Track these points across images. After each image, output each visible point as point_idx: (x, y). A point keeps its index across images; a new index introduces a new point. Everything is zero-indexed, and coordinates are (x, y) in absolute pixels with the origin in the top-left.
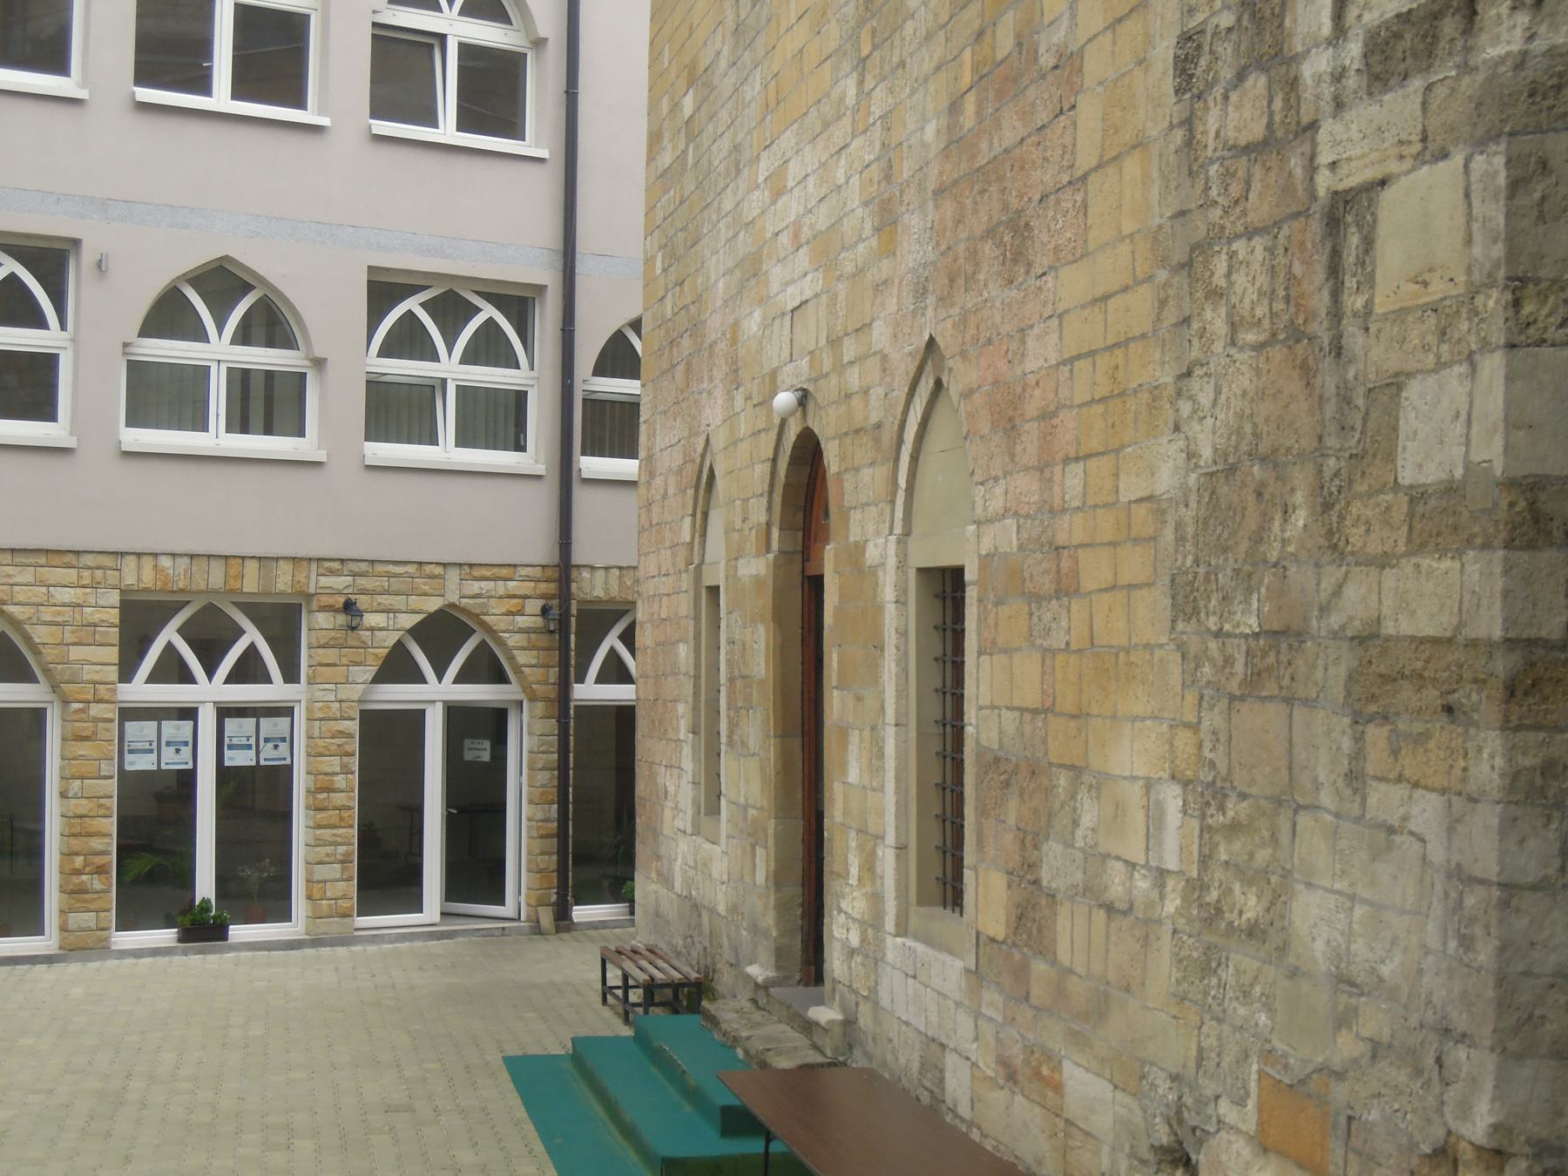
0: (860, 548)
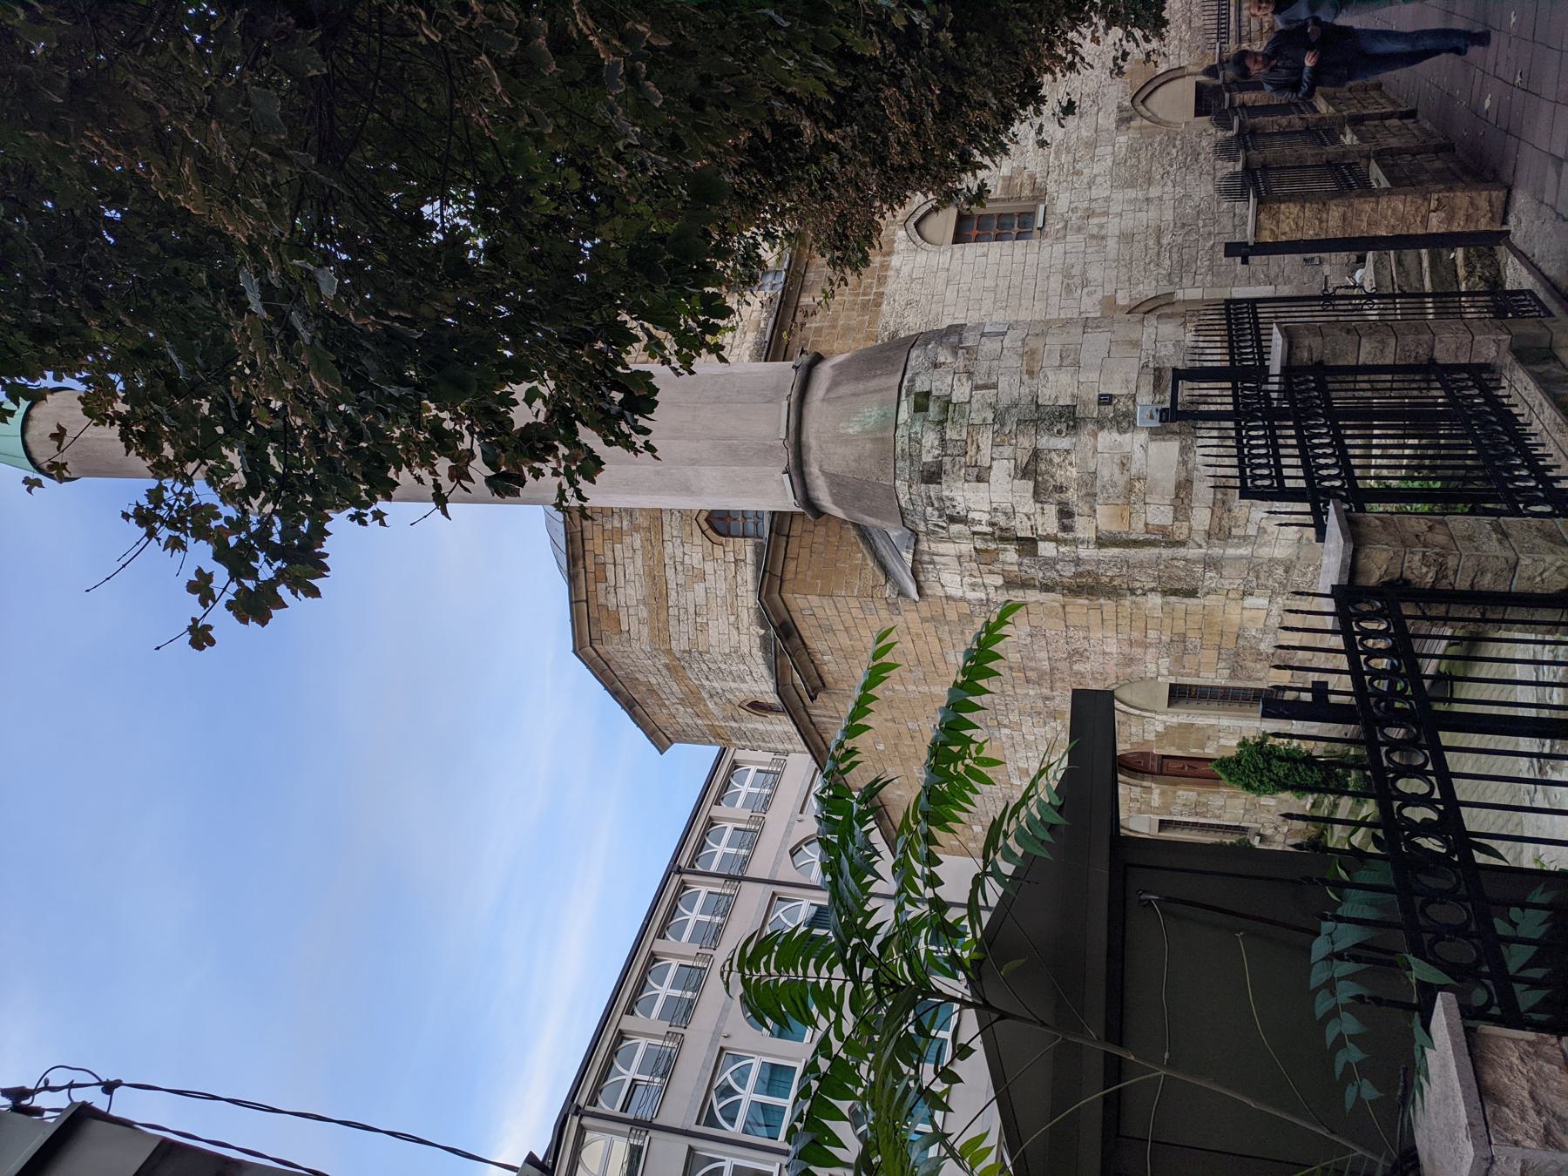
0: (1158, 734)
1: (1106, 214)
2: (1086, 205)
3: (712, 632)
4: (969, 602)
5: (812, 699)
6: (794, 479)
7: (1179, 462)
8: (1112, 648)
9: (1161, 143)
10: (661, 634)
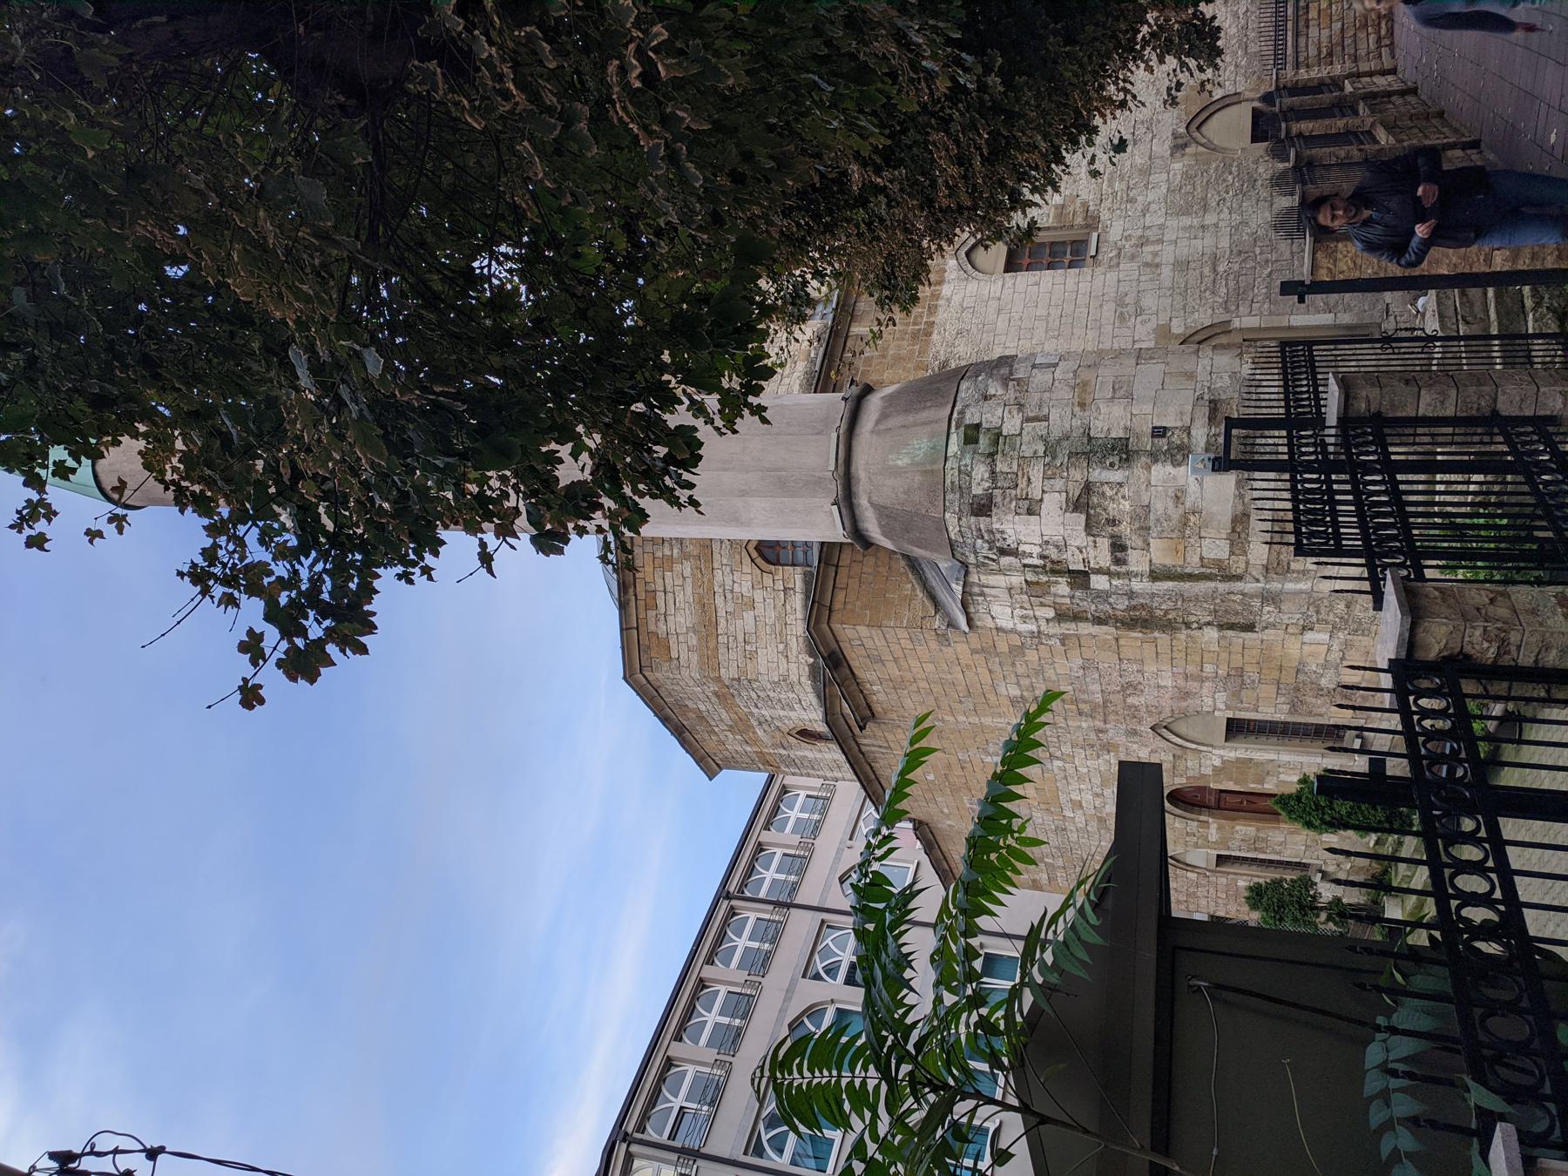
1: (1160, 241)
2: (1139, 232)
3: (762, 660)
4: (1020, 634)
5: (861, 729)
6: (843, 510)
7: (1235, 496)
8: (1168, 682)
9: (1216, 169)
10: (710, 661)
